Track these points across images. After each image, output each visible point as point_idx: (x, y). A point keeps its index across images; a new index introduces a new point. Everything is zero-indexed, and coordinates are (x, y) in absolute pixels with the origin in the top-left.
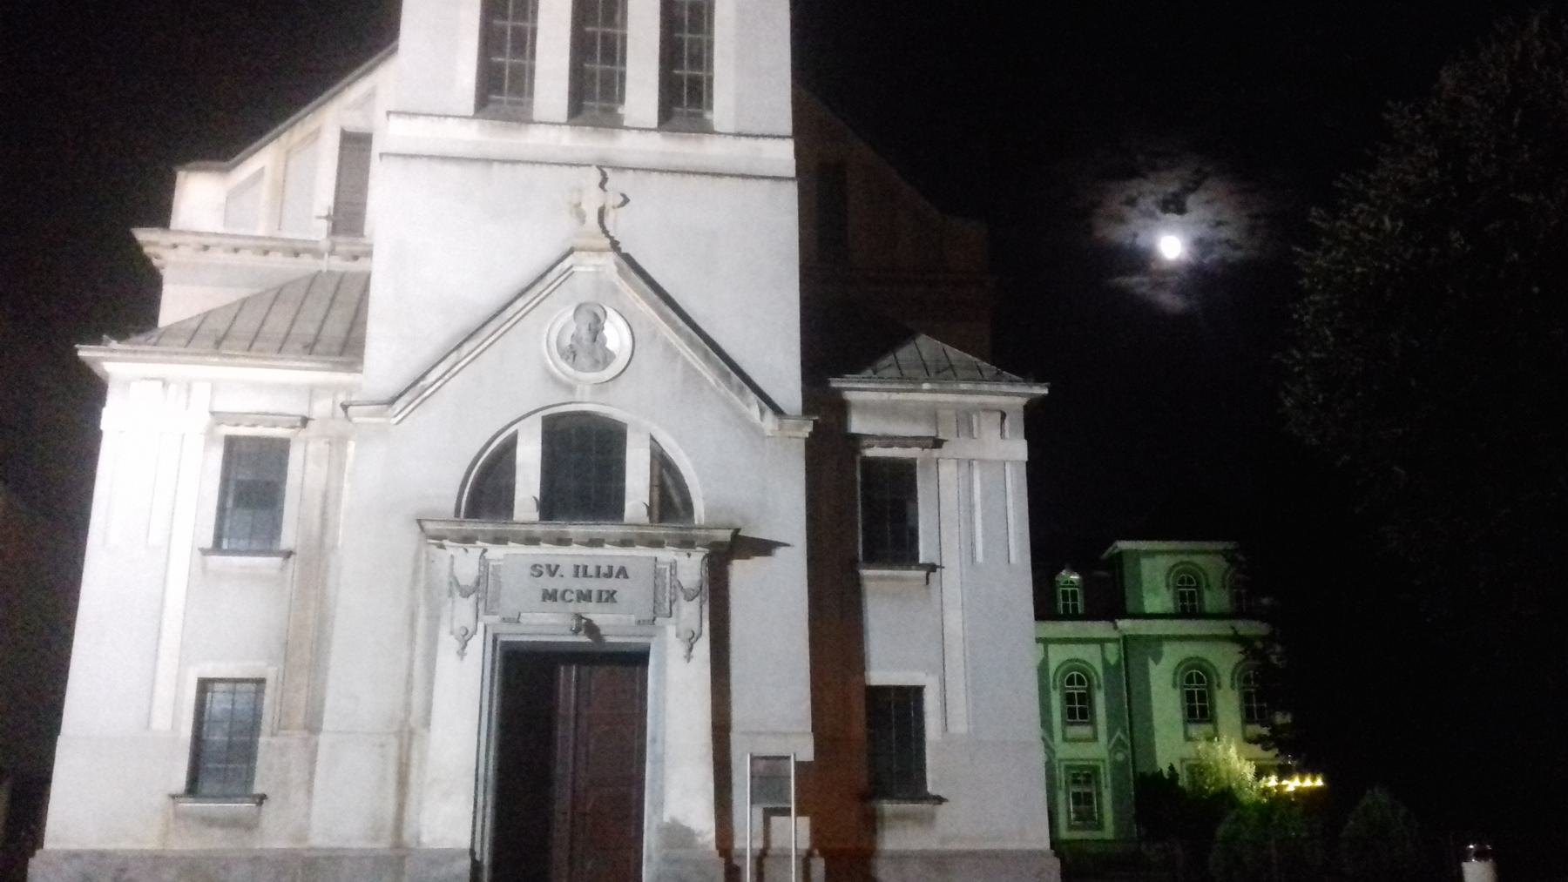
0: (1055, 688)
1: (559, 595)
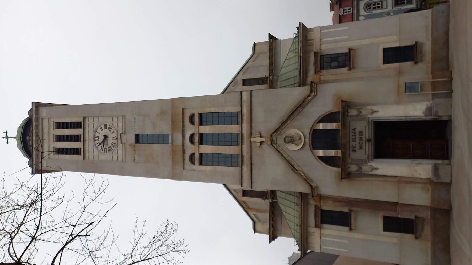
0: (372, 12)
1: (360, 145)
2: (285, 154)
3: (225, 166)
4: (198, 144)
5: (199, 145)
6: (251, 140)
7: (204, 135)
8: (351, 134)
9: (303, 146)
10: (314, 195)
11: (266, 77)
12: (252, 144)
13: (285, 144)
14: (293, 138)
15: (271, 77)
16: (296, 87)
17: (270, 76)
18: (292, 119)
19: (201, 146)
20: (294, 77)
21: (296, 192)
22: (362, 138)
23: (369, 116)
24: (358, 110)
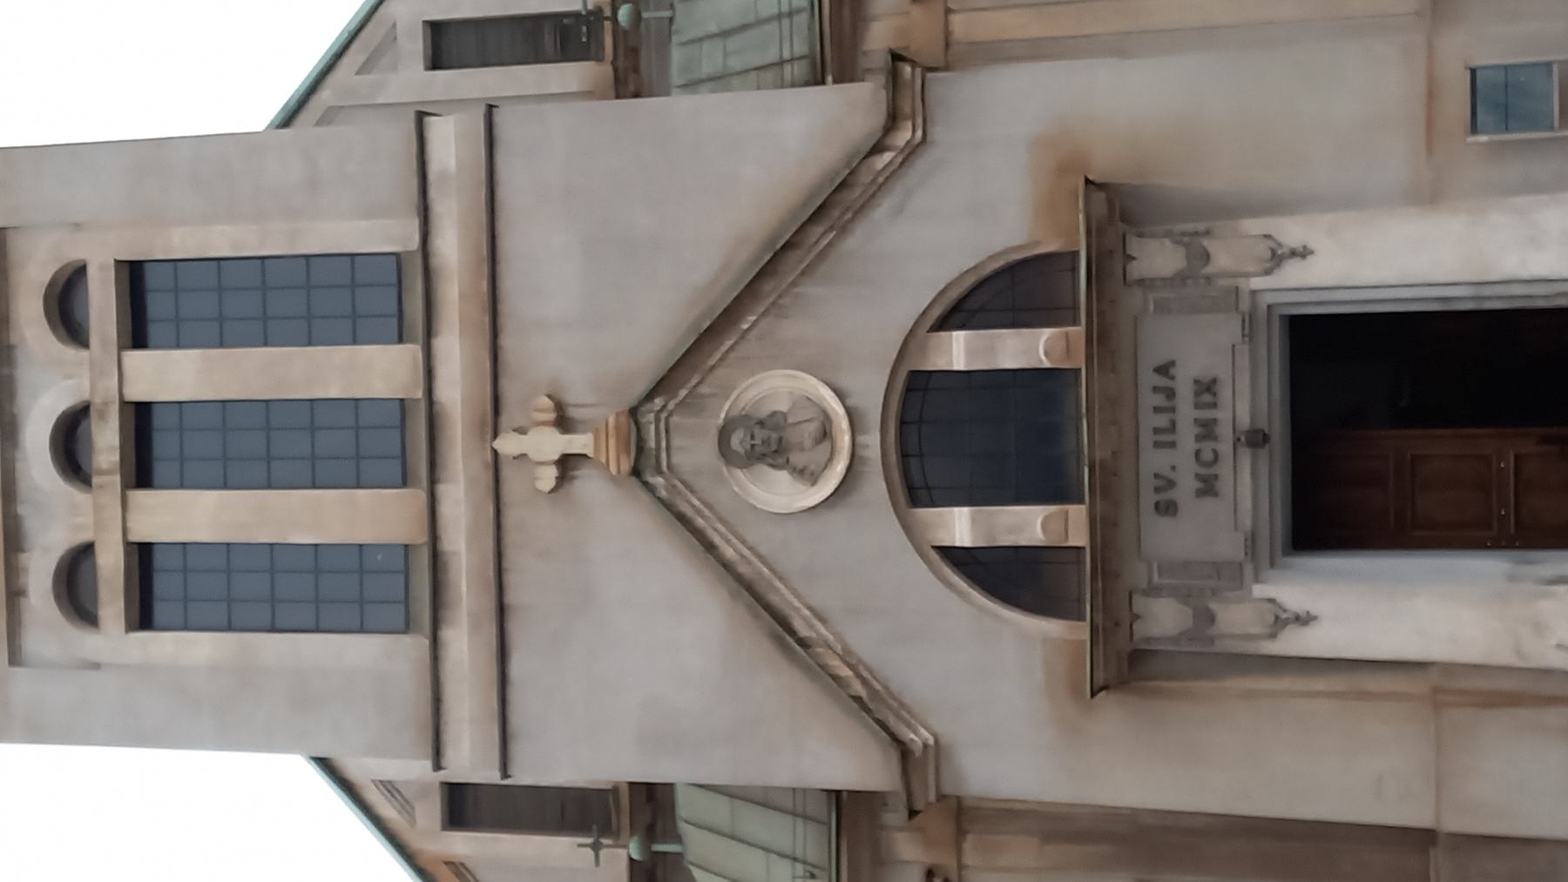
1: (1203, 471)
2: (728, 541)
3: (317, 630)
4: (117, 478)
5: (126, 486)
6: (497, 444)
7: (159, 419)
8: (1149, 400)
9: (842, 483)
10: (919, 805)
11: (590, 7)
12: (507, 472)
13: (724, 469)
14: (776, 428)
15: (624, 13)
16: (793, 85)
17: (615, 10)
18: (771, 299)
19: (139, 496)
20: (779, 17)
21: (804, 790)
22: (1215, 421)
23: (1257, 283)
24: (1186, 239)
